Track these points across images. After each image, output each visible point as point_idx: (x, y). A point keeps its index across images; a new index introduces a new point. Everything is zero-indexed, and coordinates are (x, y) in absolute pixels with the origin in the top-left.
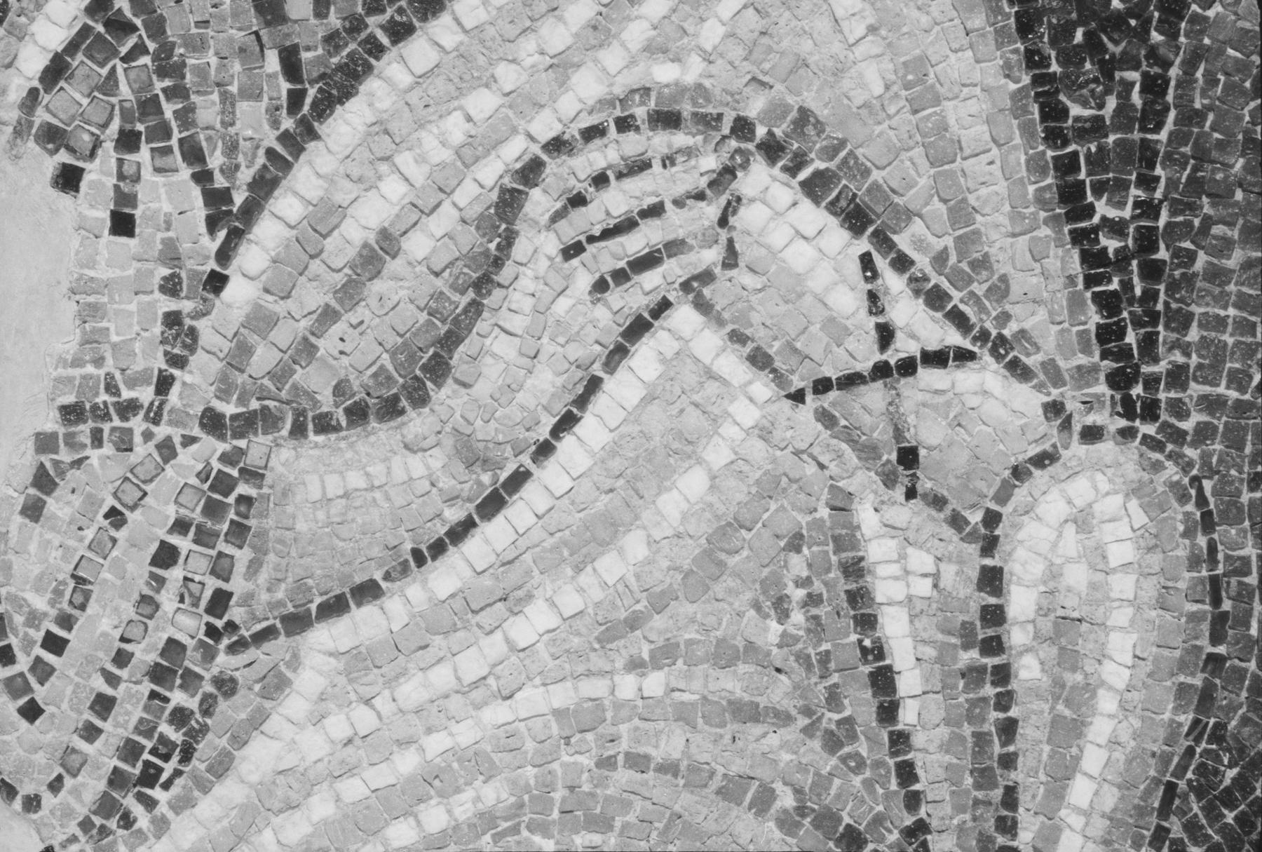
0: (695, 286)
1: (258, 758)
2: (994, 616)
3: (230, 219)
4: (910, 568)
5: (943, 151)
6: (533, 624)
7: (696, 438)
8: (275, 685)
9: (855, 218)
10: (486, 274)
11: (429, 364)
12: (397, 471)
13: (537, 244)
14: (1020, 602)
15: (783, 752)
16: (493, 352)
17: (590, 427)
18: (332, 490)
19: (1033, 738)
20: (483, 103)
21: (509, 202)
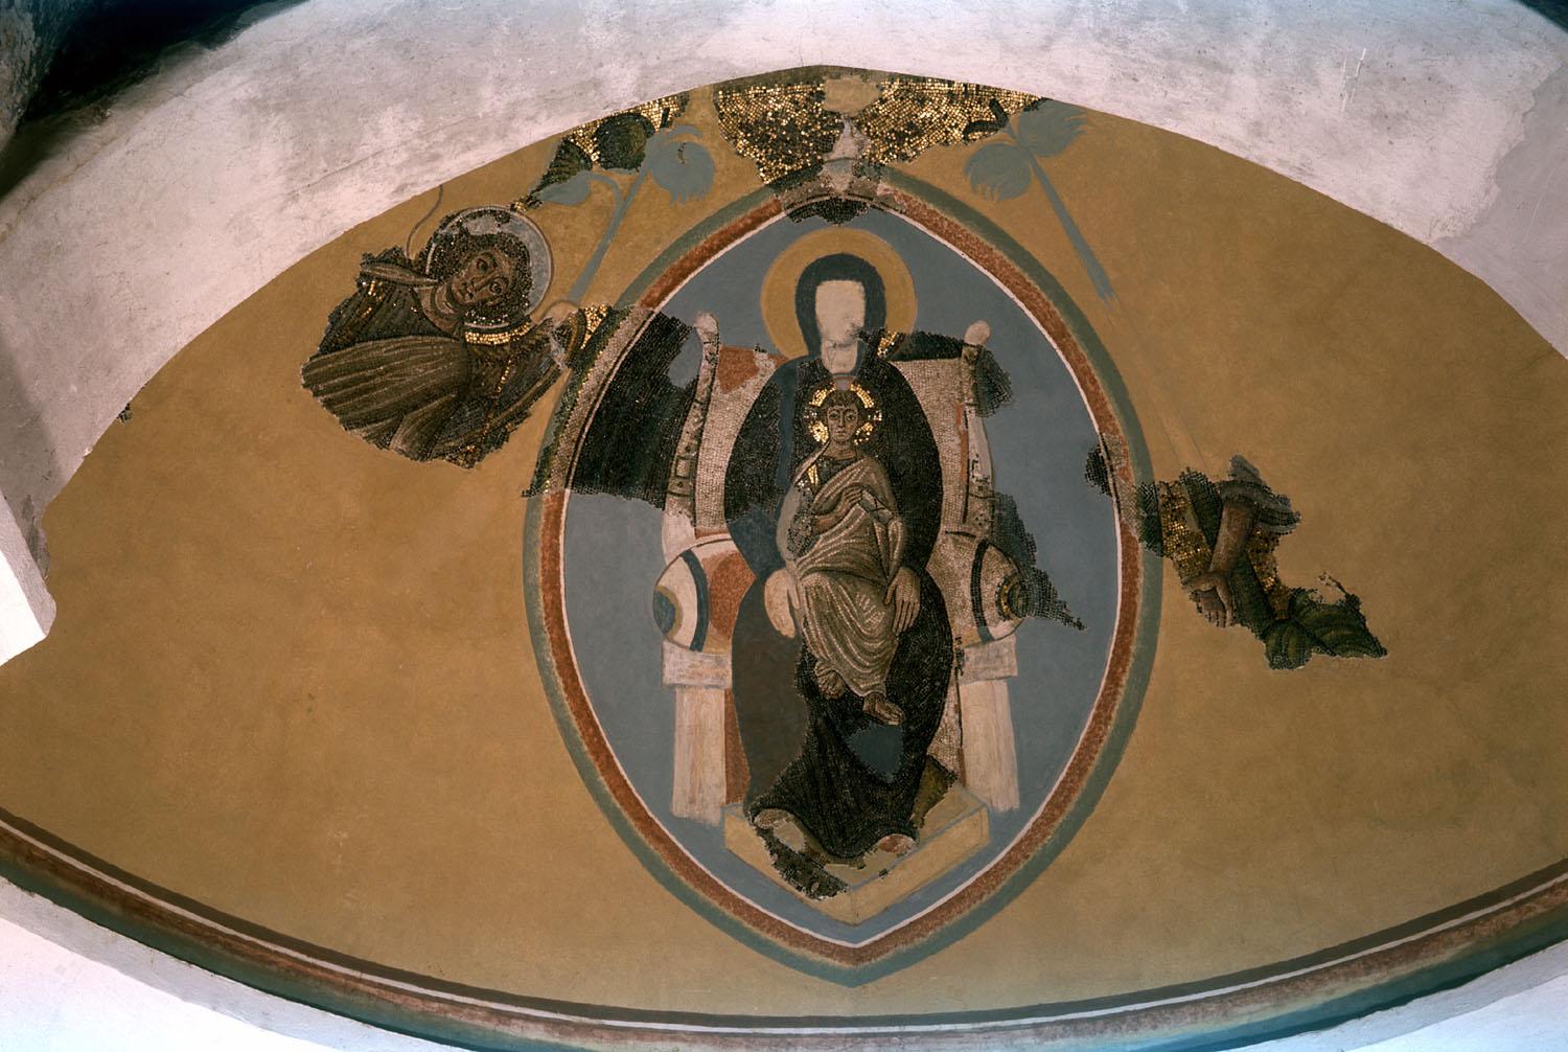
0: (859, 502)
1: (816, 546)
2: (887, 533)
3: (815, 494)
4: (878, 530)
5: (882, 488)
6: (842, 534)
7: (855, 515)
8: (817, 540)
9: (873, 495)
10: (839, 500)
11: (834, 507)
12: (830, 518)
13: (843, 498)
14: (890, 533)
15: (867, 547)
16: (839, 507)
17: (849, 515)
18: (823, 520)
19: (891, 545)
20: (839, 484)
21: (841, 493)
